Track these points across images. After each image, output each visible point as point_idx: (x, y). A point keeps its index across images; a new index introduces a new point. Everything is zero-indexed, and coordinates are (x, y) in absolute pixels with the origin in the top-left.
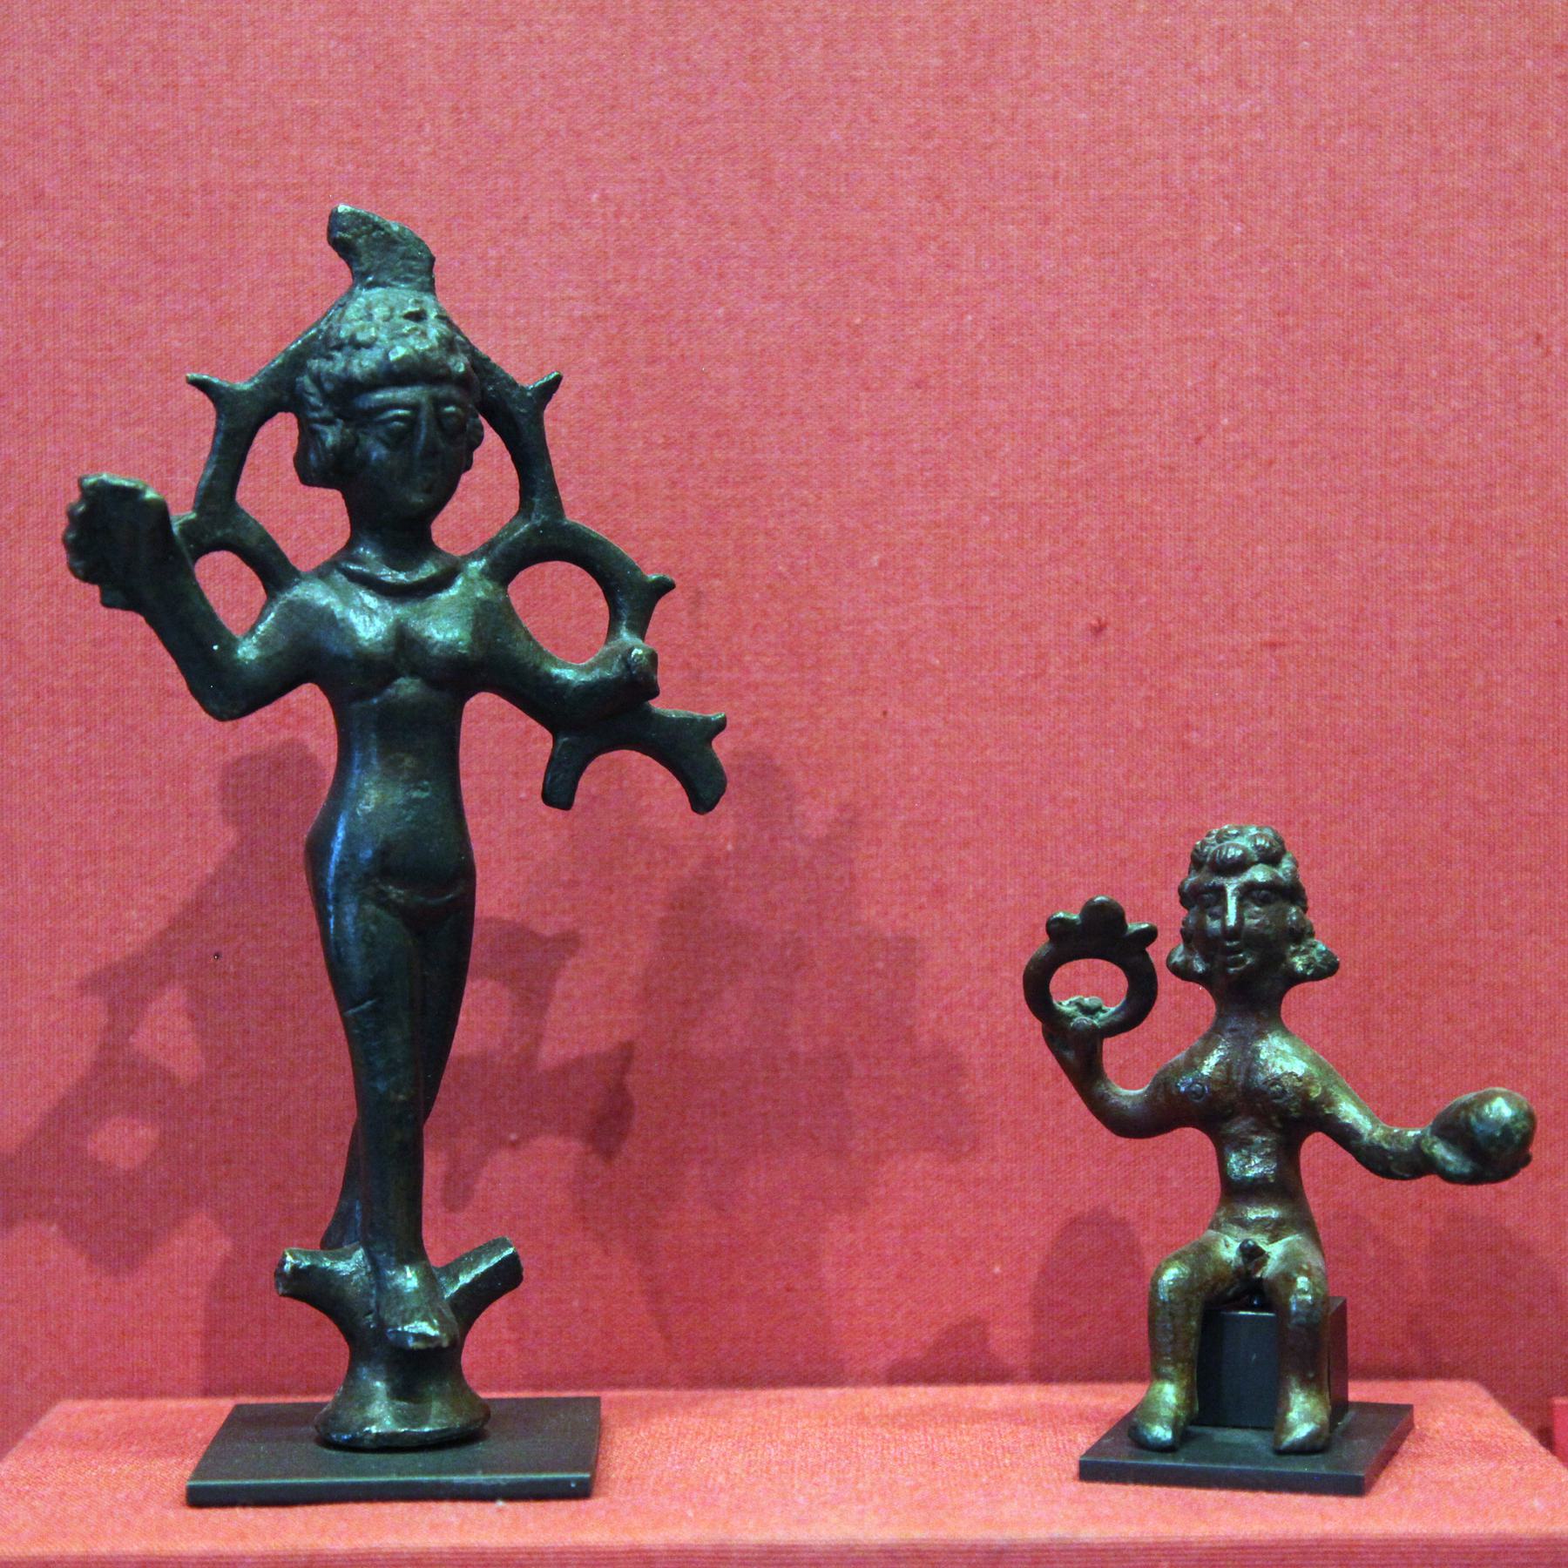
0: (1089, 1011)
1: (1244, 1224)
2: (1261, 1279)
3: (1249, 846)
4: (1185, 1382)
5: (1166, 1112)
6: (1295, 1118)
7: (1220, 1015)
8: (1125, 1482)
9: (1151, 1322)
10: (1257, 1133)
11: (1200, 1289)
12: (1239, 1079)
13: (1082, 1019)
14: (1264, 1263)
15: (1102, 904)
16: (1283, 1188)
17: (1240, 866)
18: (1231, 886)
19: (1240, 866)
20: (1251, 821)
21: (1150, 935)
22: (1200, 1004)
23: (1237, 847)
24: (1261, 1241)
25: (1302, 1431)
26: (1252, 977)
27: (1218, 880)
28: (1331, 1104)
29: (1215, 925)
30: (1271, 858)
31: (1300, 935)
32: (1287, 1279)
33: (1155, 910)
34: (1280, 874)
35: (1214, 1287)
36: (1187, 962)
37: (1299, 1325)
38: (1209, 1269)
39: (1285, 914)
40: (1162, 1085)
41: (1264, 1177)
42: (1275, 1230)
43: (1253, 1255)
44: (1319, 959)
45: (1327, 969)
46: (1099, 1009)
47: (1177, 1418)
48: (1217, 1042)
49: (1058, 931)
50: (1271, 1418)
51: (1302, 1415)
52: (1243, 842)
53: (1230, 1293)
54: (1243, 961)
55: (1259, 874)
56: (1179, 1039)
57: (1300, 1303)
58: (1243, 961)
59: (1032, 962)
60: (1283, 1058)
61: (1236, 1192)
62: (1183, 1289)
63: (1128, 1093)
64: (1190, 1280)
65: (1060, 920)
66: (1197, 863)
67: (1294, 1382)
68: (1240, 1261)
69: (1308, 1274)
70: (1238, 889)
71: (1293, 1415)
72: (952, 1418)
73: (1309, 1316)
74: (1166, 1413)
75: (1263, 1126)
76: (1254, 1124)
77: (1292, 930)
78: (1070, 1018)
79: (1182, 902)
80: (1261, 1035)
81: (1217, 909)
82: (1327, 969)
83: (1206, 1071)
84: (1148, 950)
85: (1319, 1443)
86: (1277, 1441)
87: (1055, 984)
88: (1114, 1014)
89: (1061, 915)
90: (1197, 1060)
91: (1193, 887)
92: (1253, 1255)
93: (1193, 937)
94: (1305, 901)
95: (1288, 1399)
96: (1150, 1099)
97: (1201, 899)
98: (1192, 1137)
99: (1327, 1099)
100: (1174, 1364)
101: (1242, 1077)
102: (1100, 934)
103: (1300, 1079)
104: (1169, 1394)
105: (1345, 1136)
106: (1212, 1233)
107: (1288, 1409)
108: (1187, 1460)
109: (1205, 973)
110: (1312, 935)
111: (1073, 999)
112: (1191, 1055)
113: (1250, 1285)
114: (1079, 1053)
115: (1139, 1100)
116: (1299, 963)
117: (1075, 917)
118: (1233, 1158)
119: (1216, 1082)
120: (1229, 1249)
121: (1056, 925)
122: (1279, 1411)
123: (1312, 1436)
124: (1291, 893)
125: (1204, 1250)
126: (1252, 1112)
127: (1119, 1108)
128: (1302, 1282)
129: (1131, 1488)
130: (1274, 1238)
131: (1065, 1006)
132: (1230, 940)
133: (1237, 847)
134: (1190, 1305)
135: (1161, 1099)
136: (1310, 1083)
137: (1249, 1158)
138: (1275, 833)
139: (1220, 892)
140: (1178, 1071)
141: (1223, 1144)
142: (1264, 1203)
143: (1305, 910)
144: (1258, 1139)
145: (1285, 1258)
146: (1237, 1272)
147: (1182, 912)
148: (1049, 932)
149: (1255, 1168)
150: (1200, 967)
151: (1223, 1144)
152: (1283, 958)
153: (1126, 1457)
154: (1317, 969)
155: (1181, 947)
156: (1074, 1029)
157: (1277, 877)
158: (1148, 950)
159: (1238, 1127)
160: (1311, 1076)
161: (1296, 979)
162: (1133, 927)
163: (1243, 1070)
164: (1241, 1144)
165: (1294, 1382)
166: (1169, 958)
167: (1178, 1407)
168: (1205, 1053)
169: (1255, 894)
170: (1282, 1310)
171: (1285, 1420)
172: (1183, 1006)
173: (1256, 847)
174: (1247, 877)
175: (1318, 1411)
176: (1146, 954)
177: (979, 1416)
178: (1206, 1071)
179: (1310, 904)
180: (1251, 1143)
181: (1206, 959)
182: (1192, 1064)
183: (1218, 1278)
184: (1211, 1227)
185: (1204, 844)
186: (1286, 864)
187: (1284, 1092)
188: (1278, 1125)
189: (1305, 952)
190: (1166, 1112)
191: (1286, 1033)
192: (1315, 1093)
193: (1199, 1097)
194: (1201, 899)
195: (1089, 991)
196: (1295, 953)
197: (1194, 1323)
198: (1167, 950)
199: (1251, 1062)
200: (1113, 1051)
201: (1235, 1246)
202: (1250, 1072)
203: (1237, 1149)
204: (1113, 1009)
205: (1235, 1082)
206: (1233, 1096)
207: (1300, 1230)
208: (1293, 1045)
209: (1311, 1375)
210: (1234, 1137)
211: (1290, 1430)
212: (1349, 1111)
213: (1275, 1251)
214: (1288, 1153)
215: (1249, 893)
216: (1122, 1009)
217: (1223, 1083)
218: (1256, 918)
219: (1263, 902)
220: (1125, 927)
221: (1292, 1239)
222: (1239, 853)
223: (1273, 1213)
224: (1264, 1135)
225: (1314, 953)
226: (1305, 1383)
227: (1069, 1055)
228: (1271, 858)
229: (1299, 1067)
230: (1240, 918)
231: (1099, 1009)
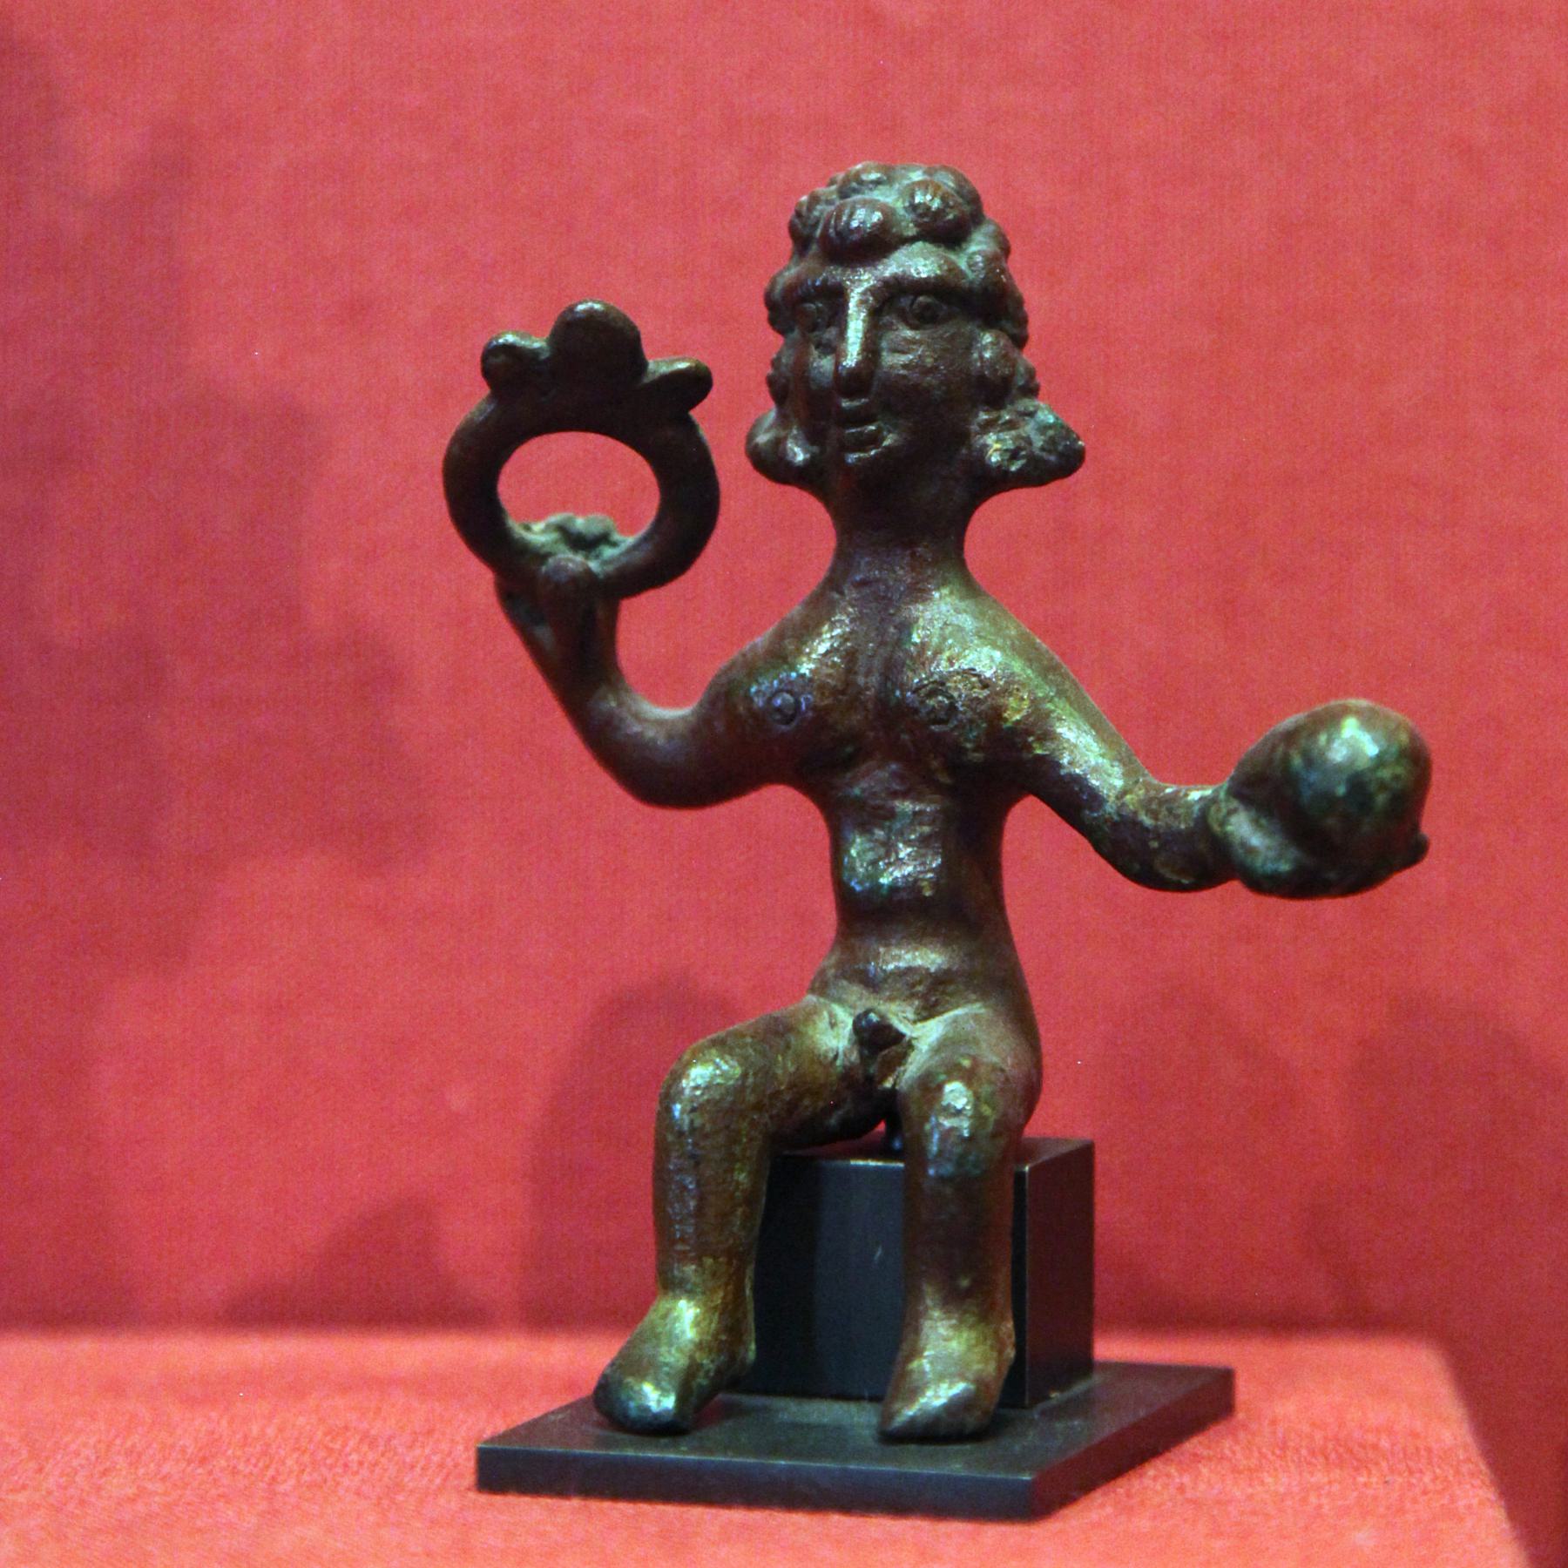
0: (585, 543)
1: (872, 983)
2: (893, 1093)
3: (899, 206)
4: (718, 1299)
5: (733, 754)
6: (986, 772)
7: (844, 558)
8: (563, 1493)
9: (661, 1177)
10: (904, 795)
11: (758, 1107)
12: (869, 682)
13: (573, 561)
14: (902, 1058)
15: (591, 314)
16: (964, 906)
17: (878, 244)
18: (861, 284)
19: (878, 244)
20: (912, 160)
21: (696, 384)
22: (809, 529)
23: (872, 205)
24: (900, 1016)
25: (938, 1396)
26: (905, 473)
27: (835, 274)
28: (1048, 736)
29: (826, 364)
30: (945, 231)
31: (998, 390)
32: (929, 1087)
33: (704, 328)
34: (962, 264)
35: (793, 1106)
36: (778, 443)
37: (942, 1179)
38: (785, 1067)
39: (971, 344)
40: (724, 700)
41: (912, 885)
42: (932, 995)
43: (878, 1041)
44: (1038, 442)
45: (1058, 463)
46: (604, 539)
47: (692, 1370)
48: (832, 608)
49: (504, 368)
50: (880, 1368)
51: (947, 1361)
52: (889, 197)
53: (833, 1121)
54: (875, 440)
55: (919, 263)
56: (763, 603)
57: (947, 1134)
58: (875, 440)
59: (458, 439)
60: (961, 642)
61: (868, 915)
62: (724, 1108)
63: (659, 714)
64: (740, 1089)
65: (509, 349)
66: (801, 240)
67: (930, 1297)
68: (854, 1057)
69: (969, 1077)
70: (871, 291)
71: (924, 1364)
72: (295, 1387)
73: (961, 1161)
74: (673, 1358)
75: (916, 782)
76: (900, 777)
77: (981, 379)
78: (541, 556)
79: (773, 322)
80: (919, 593)
81: (830, 334)
82: (1058, 463)
83: (806, 668)
84: (695, 414)
85: (972, 1421)
86: (888, 1416)
87: (510, 486)
88: (635, 547)
89: (510, 338)
90: (790, 646)
91: (790, 289)
92: (878, 1041)
93: (792, 391)
94: (1023, 321)
95: (917, 1331)
96: (702, 727)
97: (804, 312)
98: (780, 809)
99: (1039, 726)
100: (698, 1260)
101: (874, 680)
102: (588, 379)
103: (985, 684)
104: (685, 1319)
105: (1071, 799)
106: (811, 999)
107: (916, 1353)
108: (693, 1450)
109: (808, 464)
110: (1031, 391)
111: (555, 518)
112: (780, 636)
113: (869, 1103)
114: (569, 629)
115: (681, 727)
116: (995, 447)
117: (537, 343)
118: (858, 848)
119: (822, 687)
120: (833, 1034)
121: (500, 359)
122: (901, 1356)
123: (957, 1407)
124: (993, 303)
125: (781, 1032)
126: (893, 751)
127: (639, 744)
128: (956, 1094)
129: (572, 1505)
130: (928, 1011)
131: (538, 534)
132: (850, 395)
133: (872, 205)
134: (734, 1140)
135: (720, 726)
136: (1006, 692)
137: (889, 848)
138: (961, 182)
139: (836, 297)
140: (752, 670)
141: (843, 816)
142: (919, 937)
143: (1020, 341)
144: (907, 806)
145: (942, 1046)
146: (847, 1075)
147: (774, 342)
148: (488, 373)
149: (905, 865)
150: (799, 454)
151: (843, 816)
152: (963, 437)
153: (586, 1446)
154: (1033, 460)
155: (772, 415)
156: (548, 578)
157: (953, 269)
158: (695, 414)
159: (866, 783)
160: (1010, 679)
161: (992, 482)
162: (660, 365)
163: (877, 663)
164: (872, 816)
165: (930, 1297)
166: (750, 437)
167: (700, 1346)
168: (806, 630)
169: (905, 302)
170: (914, 1153)
171: (905, 1374)
172: (773, 535)
173: (914, 207)
174: (891, 267)
175: (975, 1356)
176: (691, 427)
177: (382, 1384)
178: (806, 668)
179: (1034, 328)
180: (892, 815)
181: (813, 436)
182: (780, 656)
183: (802, 1087)
184: (812, 990)
185: (815, 200)
186: (979, 246)
187: (952, 708)
188: (944, 779)
189: (1011, 425)
190: (733, 754)
191: (971, 589)
192: (1015, 713)
193: (788, 720)
194: (804, 312)
195: (582, 500)
196: (987, 427)
197: (742, 1177)
198: (736, 421)
199: (889, 645)
200: (642, 627)
201: (846, 1019)
202: (891, 669)
203: (865, 828)
204: (630, 540)
205: (861, 691)
206: (856, 718)
207: (984, 995)
208: (979, 615)
209: (965, 1283)
210: (860, 804)
211: (915, 1393)
212: (1082, 749)
213: (927, 1035)
214: (972, 839)
215: (893, 300)
216: (645, 539)
217: (835, 692)
218: (906, 352)
219: (921, 319)
220: (643, 365)
221: (966, 1013)
222: (877, 216)
223: (929, 958)
224: (918, 798)
225: (1029, 429)
226: (954, 1300)
227: (544, 634)
228: (945, 231)
229: (986, 660)
230: (871, 349)
231: (604, 539)
